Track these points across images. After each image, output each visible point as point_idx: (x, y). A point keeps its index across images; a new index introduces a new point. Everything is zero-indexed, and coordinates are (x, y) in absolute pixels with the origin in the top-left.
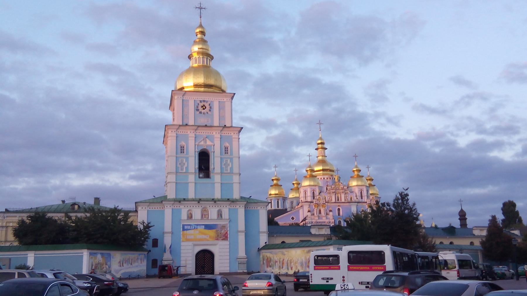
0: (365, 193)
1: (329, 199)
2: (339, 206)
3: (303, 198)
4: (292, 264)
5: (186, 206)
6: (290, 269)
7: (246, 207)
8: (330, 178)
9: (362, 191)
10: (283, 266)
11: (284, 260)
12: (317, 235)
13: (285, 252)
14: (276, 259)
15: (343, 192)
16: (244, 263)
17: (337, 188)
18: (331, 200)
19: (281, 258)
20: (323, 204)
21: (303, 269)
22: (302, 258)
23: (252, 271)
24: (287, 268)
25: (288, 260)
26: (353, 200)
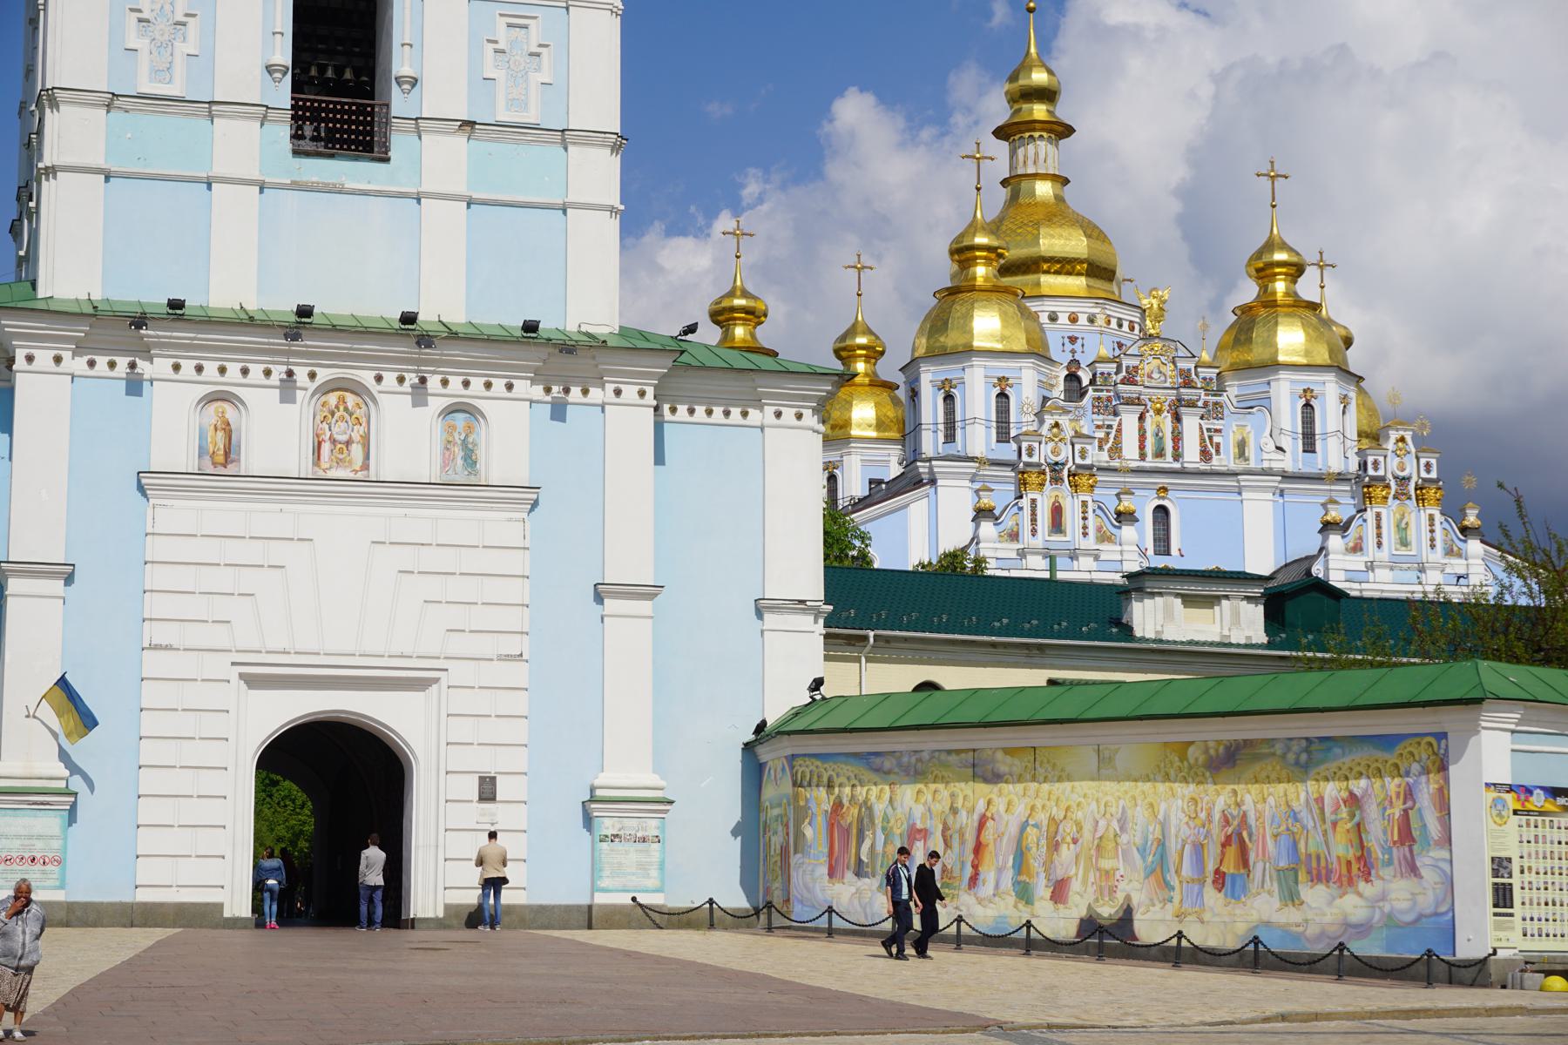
0: (1329, 416)
1: (1101, 448)
2: (1165, 489)
3: (935, 432)
4: (1066, 852)
5: (188, 367)
6: (1048, 893)
7: (666, 407)
8: (1091, 320)
9: (1313, 402)
10: (975, 867)
11: (990, 824)
12: (1175, 642)
13: (1000, 755)
14: (918, 811)
15: (1191, 404)
16: (644, 840)
17: (1156, 375)
18: (1116, 450)
19: (959, 804)
20: (1079, 467)
21: (1171, 901)
22: (1163, 807)
23: (711, 901)
24: (1016, 883)
25: (1023, 827)
26: (1253, 464)
